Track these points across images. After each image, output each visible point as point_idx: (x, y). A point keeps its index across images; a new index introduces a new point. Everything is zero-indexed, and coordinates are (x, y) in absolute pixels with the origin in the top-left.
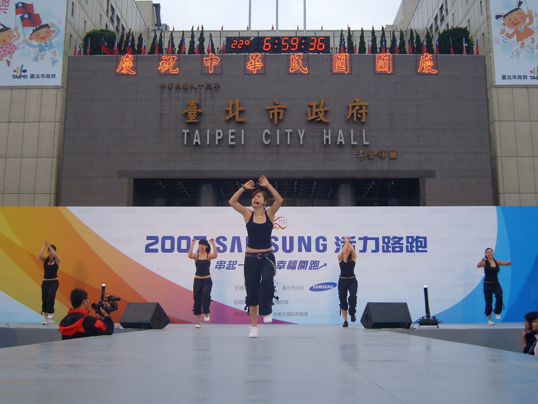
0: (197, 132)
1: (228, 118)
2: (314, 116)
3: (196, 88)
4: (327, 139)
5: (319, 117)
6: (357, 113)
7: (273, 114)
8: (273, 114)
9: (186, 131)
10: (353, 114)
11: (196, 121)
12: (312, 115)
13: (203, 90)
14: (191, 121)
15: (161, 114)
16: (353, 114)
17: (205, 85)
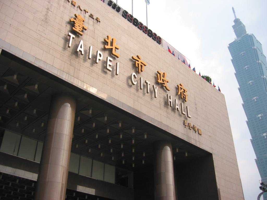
0: (82, 43)
1: (107, 47)
2: (161, 82)
3: (81, 10)
4: (170, 102)
5: (164, 84)
6: (183, 94)
7: (138, 64)
8: (138, 64)
9: (72, 36)
10: (181, 92)
11: (81, 33)
12: (160, 80)
13: (87, 15)
14: (77, 30)
15: (48, 9)
16: (181, 92)
17: (89, 14)
